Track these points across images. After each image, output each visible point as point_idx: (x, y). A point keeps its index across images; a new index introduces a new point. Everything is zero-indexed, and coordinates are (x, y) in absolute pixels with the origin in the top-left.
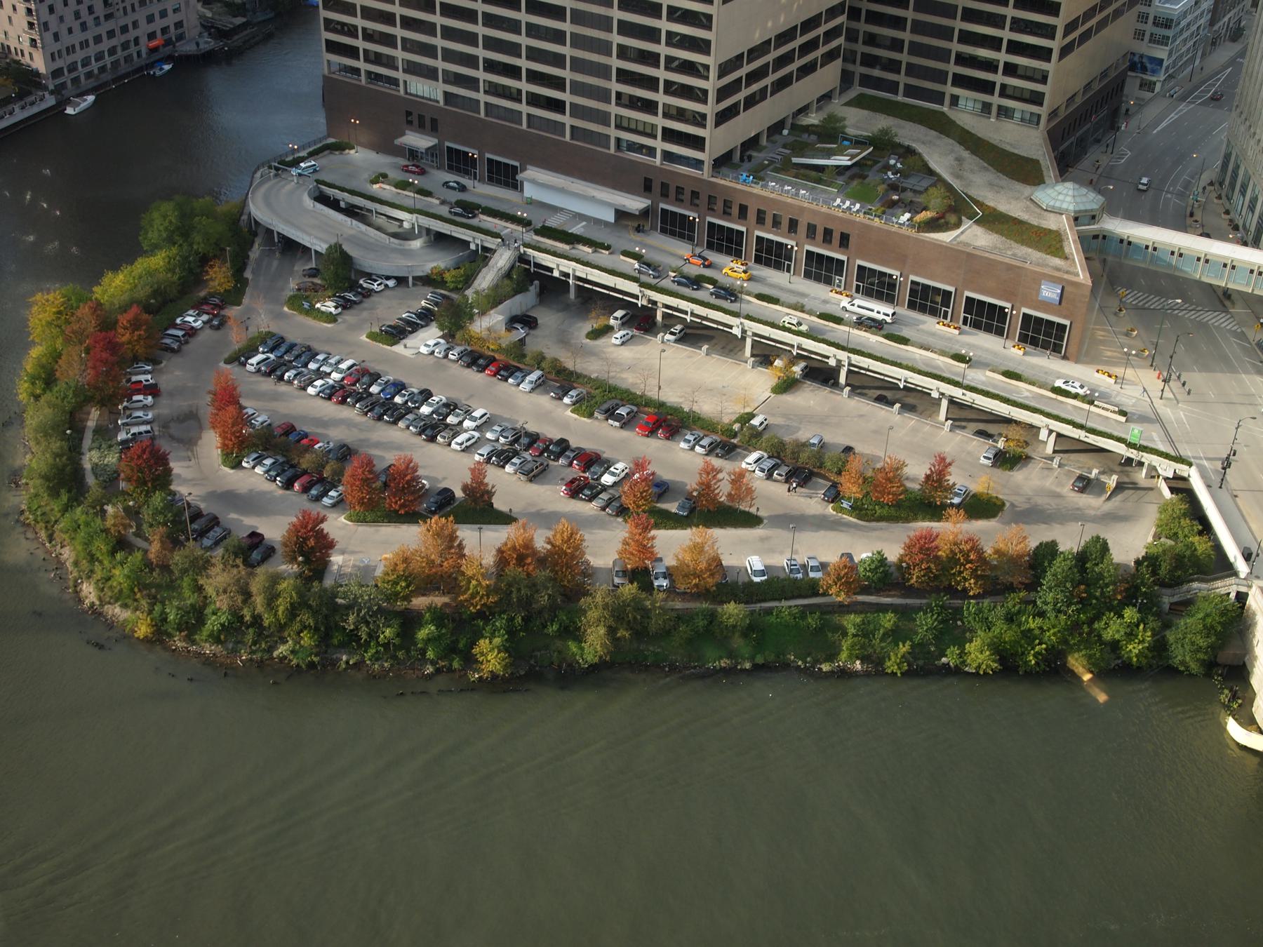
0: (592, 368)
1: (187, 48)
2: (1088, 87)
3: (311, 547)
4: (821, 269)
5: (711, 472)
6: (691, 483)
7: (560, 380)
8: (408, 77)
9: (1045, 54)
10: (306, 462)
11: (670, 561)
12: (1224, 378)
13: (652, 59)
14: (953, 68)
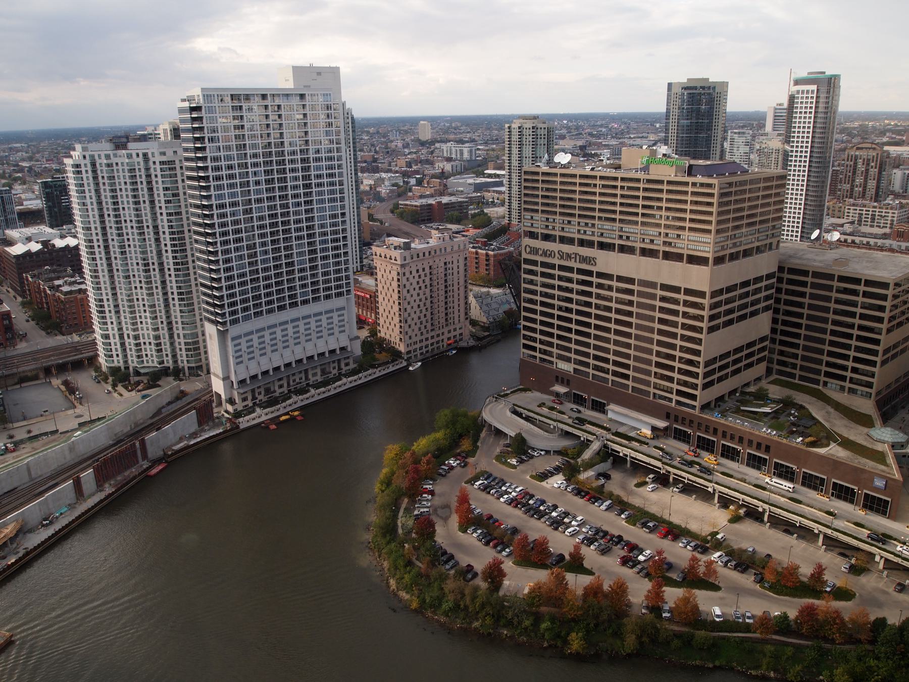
0: (636, 502)
1: (463, 344)
2: (897, 380)
3: (495, 574)
4: (756, 463)
5: (694, 559)
6: (684, 564)
7: (620, 505)
8: (558, 361)
9: (873, 364)
13: (672, 358)
14: (824, 368)
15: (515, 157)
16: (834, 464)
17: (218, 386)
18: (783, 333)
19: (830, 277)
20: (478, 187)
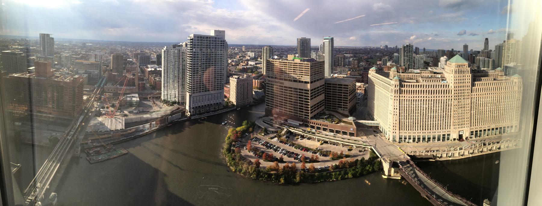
0: (296, 142)
4: (325, 130)
5: (313, 155)
7: (293, 145)
15: (265, 56)
16: (342, 127)
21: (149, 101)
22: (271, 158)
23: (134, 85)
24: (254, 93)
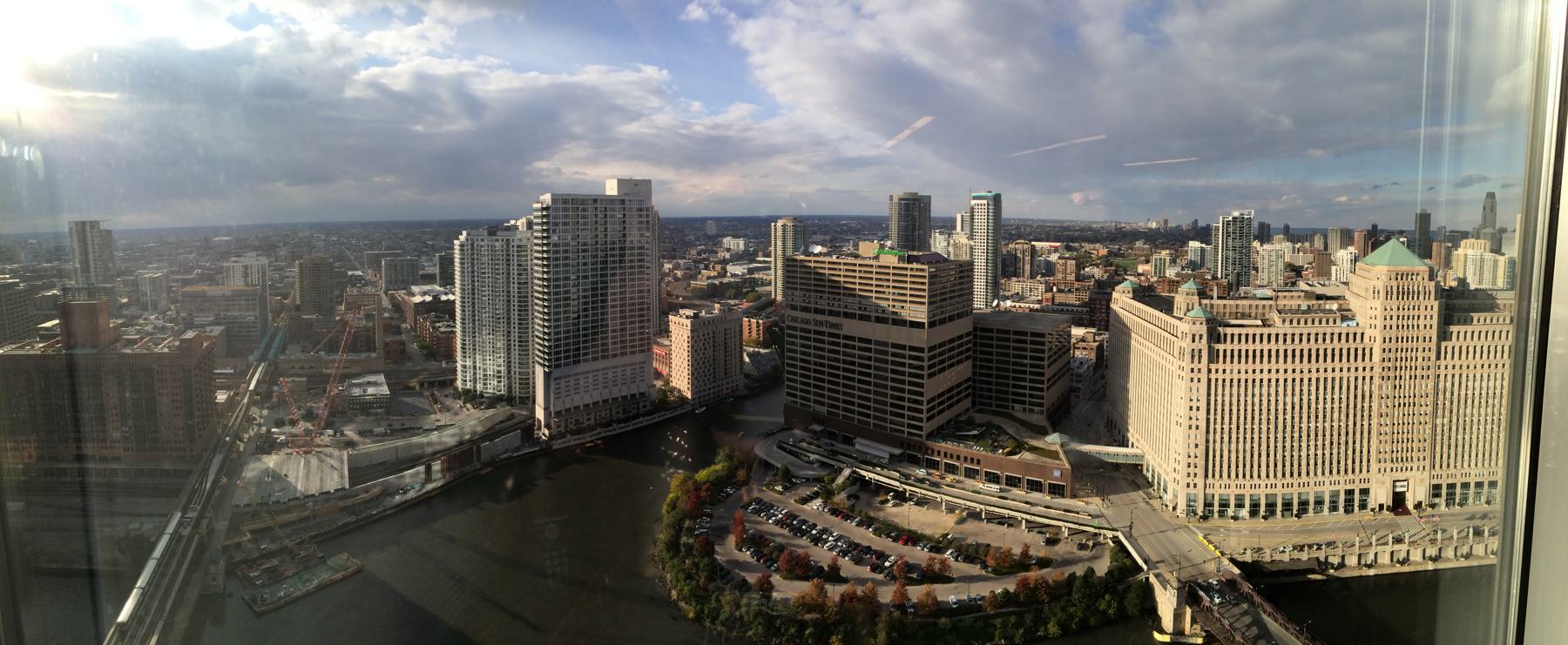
0: (881, 515)
3: (766, 587)
4: (971, 474)
5: (932, 559)
6: (924, 564)
7: (867, 522)
9: (1041, 390)
10: (766, 551)
11: (915, 600)
12: (1122, 495)
16: (1027, 466)
17: (540, 414)
18: (981, 375)
19: (1008, 332)
20: (751, 271)
21: (421, 394)
22: (801, 569)
23: (370, 347)
24: (747, 359)
